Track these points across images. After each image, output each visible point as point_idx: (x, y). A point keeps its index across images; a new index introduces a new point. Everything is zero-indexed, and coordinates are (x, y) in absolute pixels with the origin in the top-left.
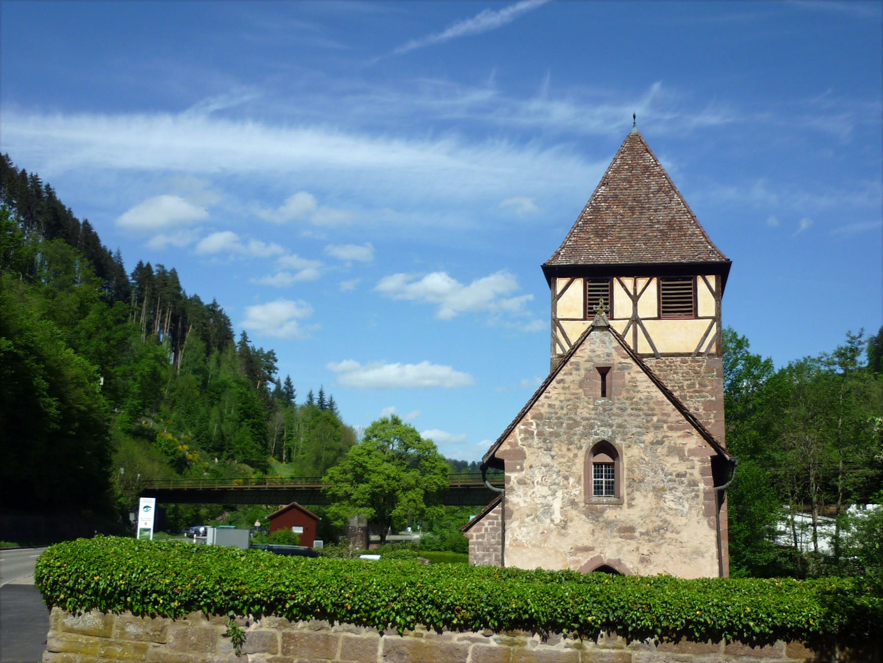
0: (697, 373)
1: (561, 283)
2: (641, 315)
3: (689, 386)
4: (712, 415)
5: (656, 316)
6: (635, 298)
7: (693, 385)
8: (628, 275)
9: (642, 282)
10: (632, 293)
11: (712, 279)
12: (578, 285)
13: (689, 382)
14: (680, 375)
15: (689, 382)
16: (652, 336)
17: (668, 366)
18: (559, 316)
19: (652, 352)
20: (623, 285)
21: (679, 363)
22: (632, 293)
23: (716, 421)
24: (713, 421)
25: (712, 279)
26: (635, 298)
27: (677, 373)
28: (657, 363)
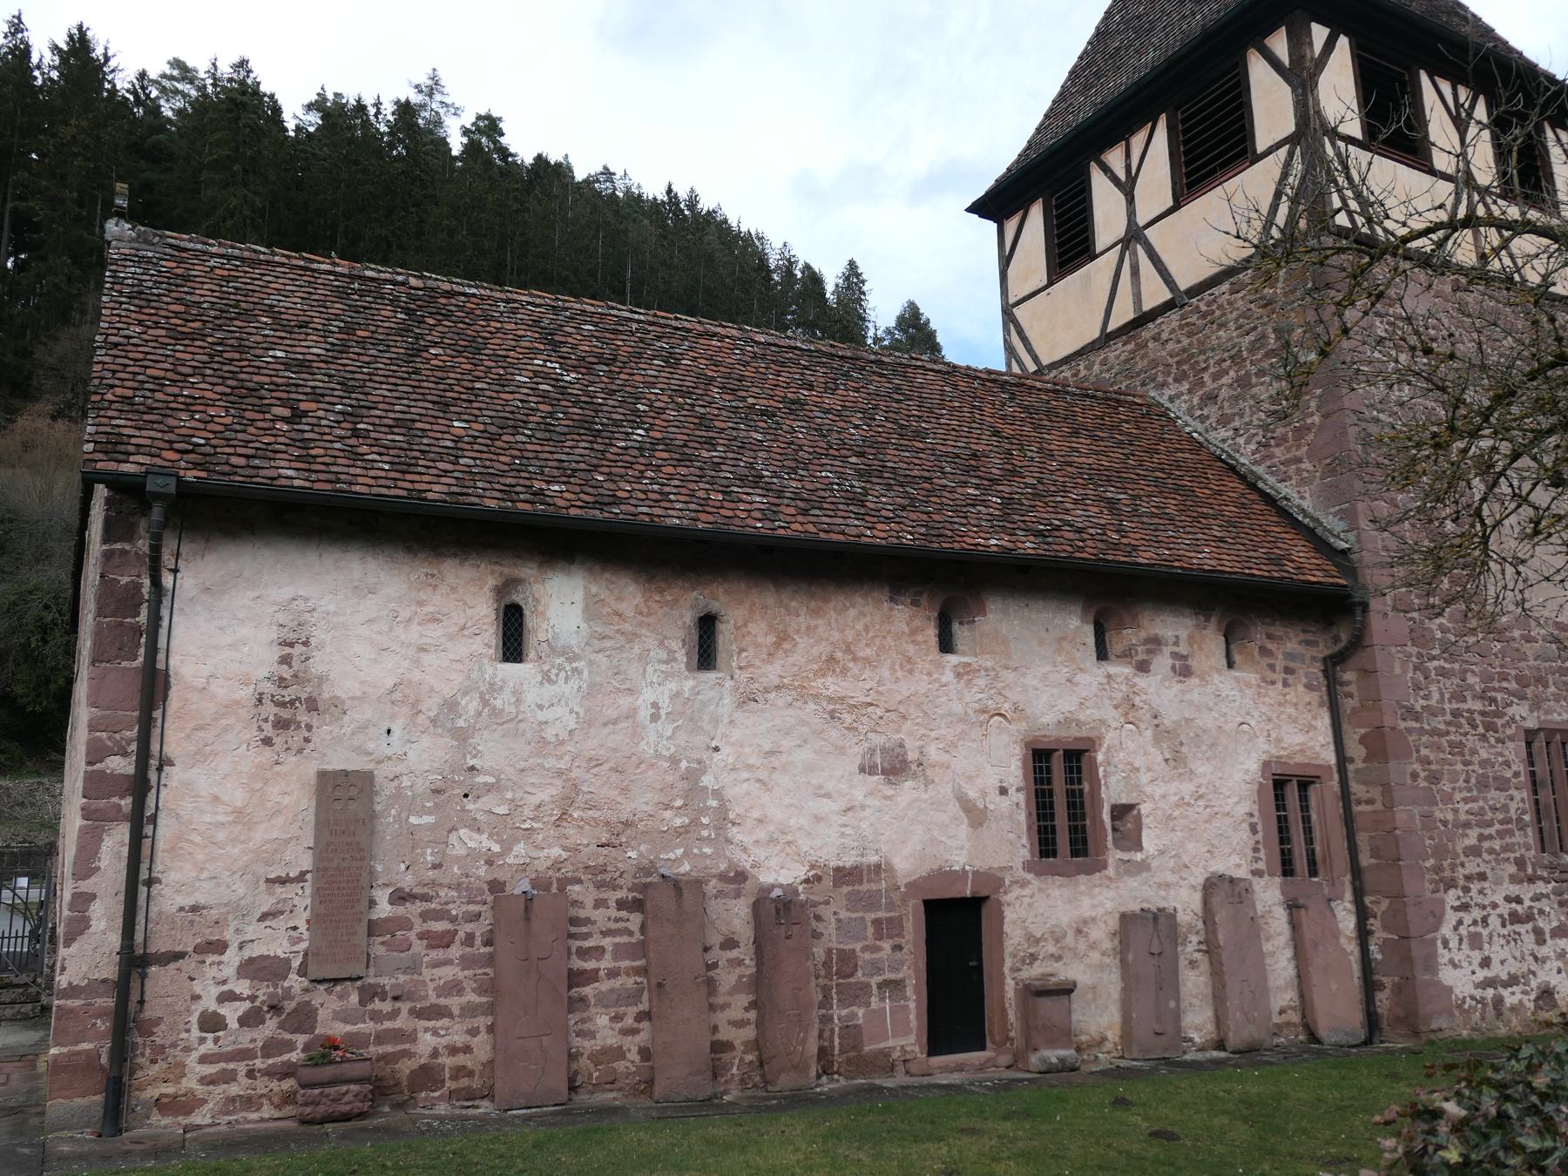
0: (1268, 303)
1: (1011, 226)
2: (1141, 221)
3: (1252, 350)
4: (1313, 404)
5: (1170, 203)
6: (1128, 187)
7: (1264, 336)
8: (1111, 144)
9: (1138, 141)
10: (1123, 177)
11: (1279, 44)
12: (1036, 217)
13: (1251, 337)
14: (1232, 325)
15: (1251, 337)
16: (1165, 258)
17: (1204, 317)
18: (1012, 300)
19: (1169, 296)
20: (1106, 169)
21: (1227, 296)
22: (1123, 177)
23: (1325, 416)
24: (1316, 419)
25: (1279, 44)
26: (1128, 187)
27: (1221, 326)
28: (1183, 318)
